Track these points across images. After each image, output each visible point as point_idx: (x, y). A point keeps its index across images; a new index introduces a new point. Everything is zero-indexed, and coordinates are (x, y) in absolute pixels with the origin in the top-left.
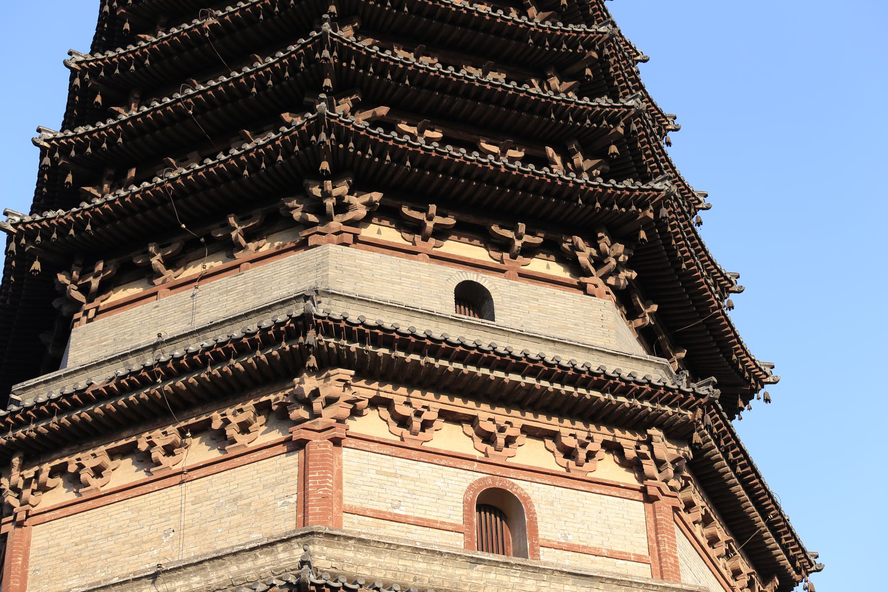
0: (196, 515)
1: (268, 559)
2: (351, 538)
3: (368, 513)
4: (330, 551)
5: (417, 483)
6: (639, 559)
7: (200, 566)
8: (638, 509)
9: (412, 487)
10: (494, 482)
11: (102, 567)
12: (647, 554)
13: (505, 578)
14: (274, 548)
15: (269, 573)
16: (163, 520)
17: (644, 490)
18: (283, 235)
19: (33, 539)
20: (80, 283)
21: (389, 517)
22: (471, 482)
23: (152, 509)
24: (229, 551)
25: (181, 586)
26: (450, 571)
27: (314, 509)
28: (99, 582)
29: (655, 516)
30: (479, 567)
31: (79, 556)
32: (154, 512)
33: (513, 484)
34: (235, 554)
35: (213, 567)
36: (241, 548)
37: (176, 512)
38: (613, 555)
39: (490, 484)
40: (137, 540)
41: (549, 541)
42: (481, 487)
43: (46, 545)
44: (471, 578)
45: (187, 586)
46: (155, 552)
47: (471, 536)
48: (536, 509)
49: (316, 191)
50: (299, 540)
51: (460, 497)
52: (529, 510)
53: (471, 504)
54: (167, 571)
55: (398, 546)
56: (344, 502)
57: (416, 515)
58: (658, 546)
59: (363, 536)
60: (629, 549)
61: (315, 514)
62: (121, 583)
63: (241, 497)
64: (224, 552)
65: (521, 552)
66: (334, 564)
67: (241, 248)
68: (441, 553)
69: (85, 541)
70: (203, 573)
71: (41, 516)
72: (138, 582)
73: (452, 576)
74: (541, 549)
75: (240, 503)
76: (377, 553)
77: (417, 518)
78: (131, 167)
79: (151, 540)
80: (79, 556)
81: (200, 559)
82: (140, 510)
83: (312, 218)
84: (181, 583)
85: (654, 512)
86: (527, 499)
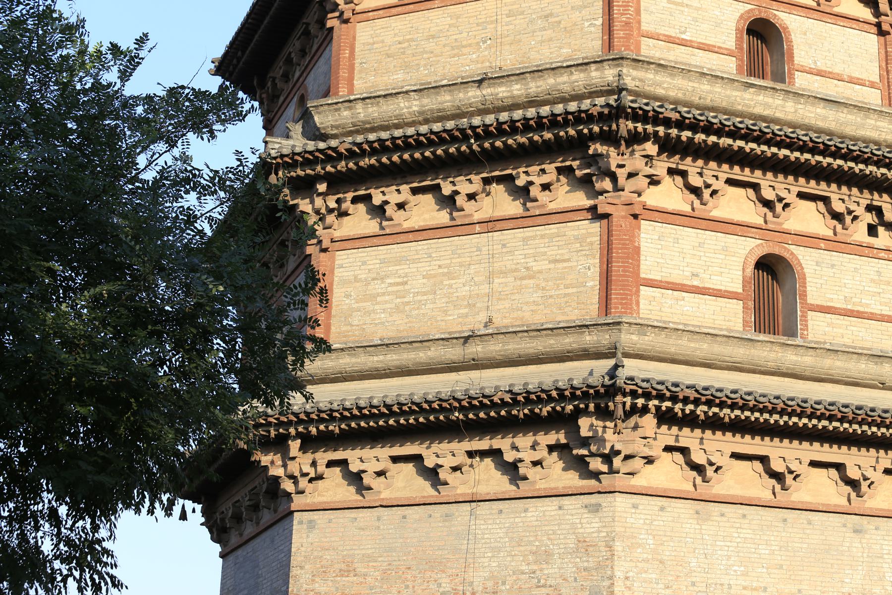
0: (512, 27)
1: (582, 75)
2: (652, 63)
3: (661, 37)
4: (634, 73)
5: (700, 12)
6: (872, 85)
7: (522, 76)
8: (872, 40)
9: (695, 15)
10: (760, 12)
11: (425, 65)
12: (878, 81)
13: (770, 100)
14: (588, 67)
15: (581, 87)
16: (480, 28)
17: (878, 25)
19: (358, 35)
21: (677, 41)
22: (742, 12)
23: (470, 17)
24: (548, 66)
25: (504, 92)
26: (728, 92)
27: (618, 33)
28: (430, 83)
29: (886, 48)
30: (751, 90)
31: (403, 53)
32: (471, 20)
33: (775, 15)
34: (553, 69)
35: (533, 78)
36: (559, 64)
37: (492, 22)
38: (852, 81)
39: (757, 15)
40: (457, 44)
41: (802, 66)
42: (750, 17)
43: (371, 41)
44: (744, 99)
45: (508, 91)
46: (474, 56)
47: (742, 60)
48: (793, 36)
50: (610, 62)
51: (733, 25)
52: (787, 38)
53: (742, 32)
54: (492, 78)
55: (689, 71)
56: (642, 28)
57: (699, 40)
58: (888, 75)
59: (662, 62)
60: (864, 76)
61: (620, 38)
62: (449, 85)
63: (551, 15)
64: (544, 67)
65: (779, 77)
66: (637, 83)
68: (722, 78)
69: (408, 41)
70: (524, 82)
71: (365, 15)
72: (465, 85)
73: (729, 97)
74: (796, 73)
75: (550, 20)
76: (672, 76)
77: (700, 43)
79: (470, 45)
80: (403, 53)
81: (522, 71)
82: (458, 18)
84: (504, 89)
85: (886, 45)
86: (786, 28)
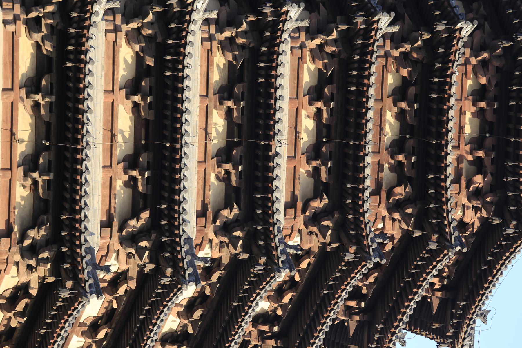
18: (29, 206)
20: (43, 22)
49: (44, 255)
67: (26, 175)
78: (155, 62)
83: (27, 242)
